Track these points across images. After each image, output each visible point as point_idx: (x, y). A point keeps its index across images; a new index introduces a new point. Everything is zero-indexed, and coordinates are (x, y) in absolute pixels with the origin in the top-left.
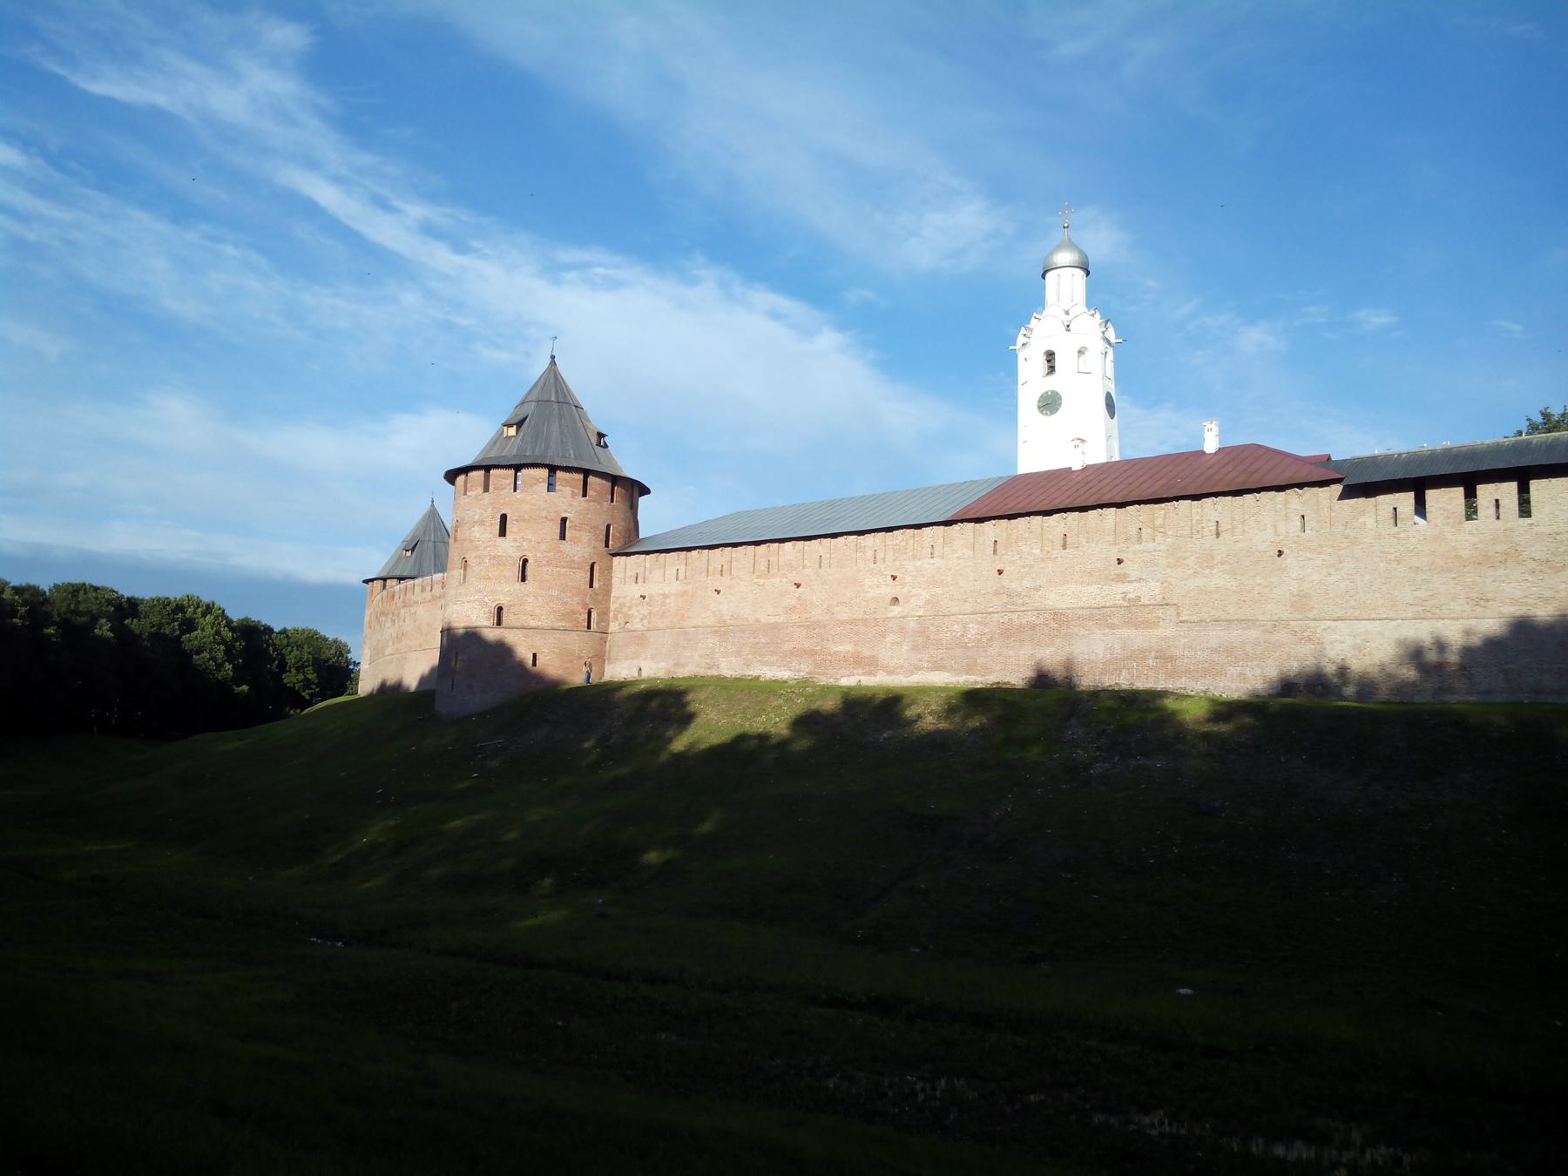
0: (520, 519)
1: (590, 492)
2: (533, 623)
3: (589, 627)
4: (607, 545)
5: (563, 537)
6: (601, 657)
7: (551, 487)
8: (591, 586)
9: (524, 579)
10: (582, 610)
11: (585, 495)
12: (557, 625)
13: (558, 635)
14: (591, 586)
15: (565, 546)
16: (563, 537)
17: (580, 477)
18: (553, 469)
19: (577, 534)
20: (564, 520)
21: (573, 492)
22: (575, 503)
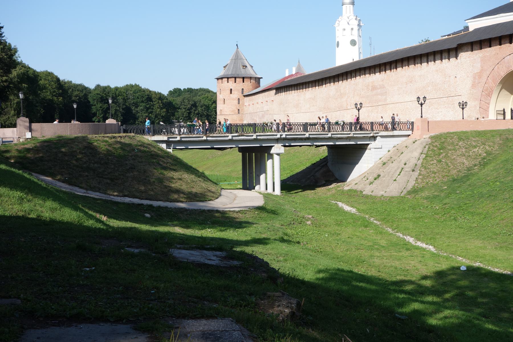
0: (223, 90)
1: (237, 82)
2: (226, 114)
3: (239, 113)
4: (243, 93)
5: (231, 93)
6: (242, 120)
7: (228, 82)
8: (239, 103)
9: (224, 104)
10: (236, 109)
11: (235, 82)
12: (230, 114)
13: (231, 116)
14: (239, 103)
15: (231, 95)
16: (231, 93)
17: (234, 79)
18: (228, 78)
19: (234, 92)
20: (231, 89)
21: (233, 83)
22: (233, 85)
